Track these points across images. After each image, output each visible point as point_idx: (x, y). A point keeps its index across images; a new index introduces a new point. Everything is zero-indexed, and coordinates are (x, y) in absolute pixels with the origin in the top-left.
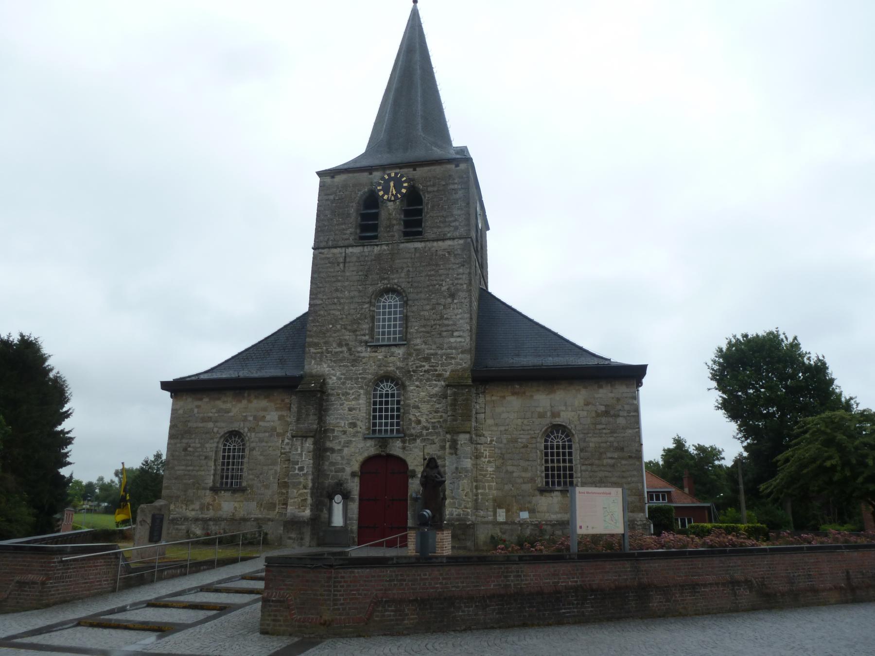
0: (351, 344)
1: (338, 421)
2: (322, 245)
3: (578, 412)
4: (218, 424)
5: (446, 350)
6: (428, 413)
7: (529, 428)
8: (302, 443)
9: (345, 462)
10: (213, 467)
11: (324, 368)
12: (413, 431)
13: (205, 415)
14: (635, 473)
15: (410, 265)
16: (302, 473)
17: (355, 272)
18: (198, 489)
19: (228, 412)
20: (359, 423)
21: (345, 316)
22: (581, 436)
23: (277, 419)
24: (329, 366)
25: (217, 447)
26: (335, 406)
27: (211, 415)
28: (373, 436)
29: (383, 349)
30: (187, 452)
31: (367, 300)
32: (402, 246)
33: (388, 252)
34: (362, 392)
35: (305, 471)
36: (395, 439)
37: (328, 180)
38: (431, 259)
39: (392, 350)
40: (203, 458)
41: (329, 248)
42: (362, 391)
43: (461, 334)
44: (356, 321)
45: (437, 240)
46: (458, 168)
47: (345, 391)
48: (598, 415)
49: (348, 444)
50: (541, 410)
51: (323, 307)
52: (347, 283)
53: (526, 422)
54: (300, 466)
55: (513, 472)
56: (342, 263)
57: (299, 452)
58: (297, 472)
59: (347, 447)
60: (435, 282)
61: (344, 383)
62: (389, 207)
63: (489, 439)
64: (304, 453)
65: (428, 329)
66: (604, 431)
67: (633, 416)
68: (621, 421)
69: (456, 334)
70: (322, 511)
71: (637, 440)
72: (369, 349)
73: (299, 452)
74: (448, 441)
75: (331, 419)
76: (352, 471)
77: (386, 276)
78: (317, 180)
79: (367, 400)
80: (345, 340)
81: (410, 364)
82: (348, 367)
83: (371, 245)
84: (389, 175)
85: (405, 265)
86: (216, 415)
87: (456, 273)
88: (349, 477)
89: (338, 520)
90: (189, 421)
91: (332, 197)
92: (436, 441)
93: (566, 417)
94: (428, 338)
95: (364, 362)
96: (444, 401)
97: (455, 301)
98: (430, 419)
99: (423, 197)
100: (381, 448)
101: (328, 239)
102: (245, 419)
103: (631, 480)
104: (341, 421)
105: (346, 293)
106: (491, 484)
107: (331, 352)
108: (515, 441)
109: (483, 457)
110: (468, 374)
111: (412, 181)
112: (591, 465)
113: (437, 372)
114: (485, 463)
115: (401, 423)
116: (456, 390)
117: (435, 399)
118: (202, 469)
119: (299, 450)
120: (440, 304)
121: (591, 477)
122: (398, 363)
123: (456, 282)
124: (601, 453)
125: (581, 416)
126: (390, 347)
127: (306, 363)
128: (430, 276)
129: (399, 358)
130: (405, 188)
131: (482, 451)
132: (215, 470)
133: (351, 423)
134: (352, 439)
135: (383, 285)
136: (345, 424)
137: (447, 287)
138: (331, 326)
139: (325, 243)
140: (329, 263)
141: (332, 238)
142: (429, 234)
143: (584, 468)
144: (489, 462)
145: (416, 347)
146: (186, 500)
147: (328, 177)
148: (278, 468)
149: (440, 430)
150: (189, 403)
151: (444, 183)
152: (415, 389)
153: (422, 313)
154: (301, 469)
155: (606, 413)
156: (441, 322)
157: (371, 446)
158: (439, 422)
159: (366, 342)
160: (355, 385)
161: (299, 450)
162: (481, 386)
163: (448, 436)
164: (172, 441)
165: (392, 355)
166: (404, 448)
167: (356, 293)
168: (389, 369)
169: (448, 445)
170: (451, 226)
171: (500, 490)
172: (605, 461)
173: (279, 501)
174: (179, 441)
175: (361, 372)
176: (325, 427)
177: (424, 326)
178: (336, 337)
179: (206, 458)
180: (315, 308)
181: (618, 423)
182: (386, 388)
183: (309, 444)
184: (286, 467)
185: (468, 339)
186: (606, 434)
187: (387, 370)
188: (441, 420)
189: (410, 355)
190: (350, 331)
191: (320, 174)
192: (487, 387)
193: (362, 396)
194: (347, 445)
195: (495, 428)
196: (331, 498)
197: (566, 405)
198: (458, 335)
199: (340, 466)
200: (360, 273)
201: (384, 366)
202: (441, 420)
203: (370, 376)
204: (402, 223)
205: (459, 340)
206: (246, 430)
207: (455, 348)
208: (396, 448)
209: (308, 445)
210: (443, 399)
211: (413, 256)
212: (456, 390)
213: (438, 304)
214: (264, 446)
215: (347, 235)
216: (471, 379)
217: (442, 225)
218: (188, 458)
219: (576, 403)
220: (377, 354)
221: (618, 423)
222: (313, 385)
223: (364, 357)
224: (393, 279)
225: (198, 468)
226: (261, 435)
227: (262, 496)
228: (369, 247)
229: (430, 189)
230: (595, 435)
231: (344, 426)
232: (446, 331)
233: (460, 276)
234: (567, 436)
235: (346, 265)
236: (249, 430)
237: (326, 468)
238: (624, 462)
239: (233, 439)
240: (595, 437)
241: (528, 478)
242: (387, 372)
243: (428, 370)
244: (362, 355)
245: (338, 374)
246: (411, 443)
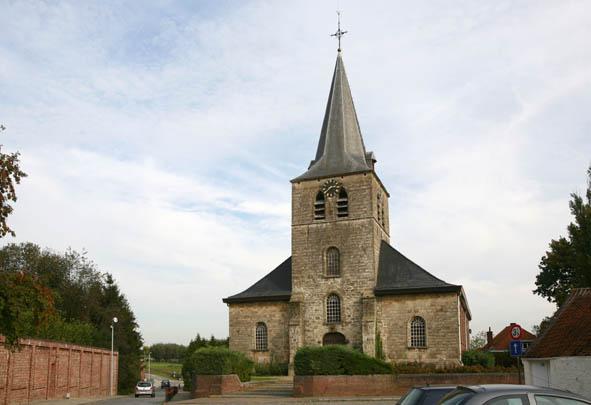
11: (302, 290)
78: (291, 185)
93: (422, 313)
108: (396, 324)
142: (352, 215)
150: (237, 309)
155: (441, 310)
208: (339, 329)
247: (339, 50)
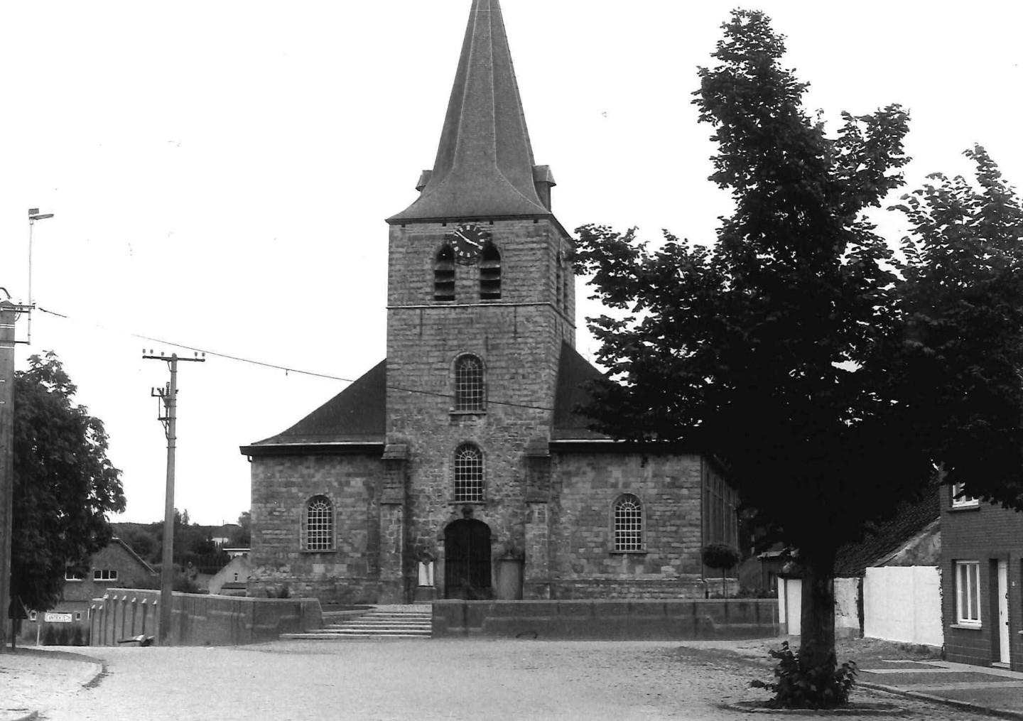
46: (536, 224)
84: (464, 228)
93: (634, 487)
115: (484, 490)
123: (534, 351)
140: (406, 325)
172: (669, 529)
208: (480, 515)
233: (539, 346)
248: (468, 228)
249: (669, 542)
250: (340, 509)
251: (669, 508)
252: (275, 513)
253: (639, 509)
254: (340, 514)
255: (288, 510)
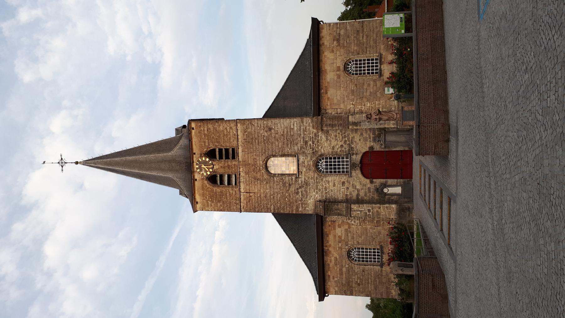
0: (297, 186)
1: (341, 192)
2: (238, 207)
3: (337, 56)
4: (344, 264)
5: (301, 132)
6: (337, 141)
7: (345, 84)
8: (354, 211)
9: (364, 187)
10: (369, 267)
12: (347, 149)
13: (338, 273)
14: (371, 24)
15: (252, 154)
16: (371, 210)
17: (255, 186)
18: (382, 275)
19: (337, 259)
20: (343, 180)
21: (281, 191)
22: (350, 54)
23: (340, 229)
24: (310, 199)
25: (357, 265)
26: (333, 194)
27: (338, 270)
28: (350, 172)
29: (300, 168)
30: (361, 283)
31: (272, 178)
32: (240, 159)
33: (244, 168)
34: (325, 179)
35: (371, 208)
36: (351, 160)
37: (198, 206)
38: (249, 142)
39: (301, 163)
40: (363, 273)
41: (240, 203)
42: (324, 179)
43: (292, 124)
44: (284, 184)
45: (238, 139)
46: (195, 128)
47: (324, 189)
48: (339, 45)
49: (354, 186)
50: (336, 77)
51: (276, 204)
52: (262, 191)
53: (342, 86)
54: (367, 212)
55: (370, 92)
56: (250, 194)
57: (359, 212)
58: (371, 213)
59: (356, 186)
60: (262, 139)
61: (320, 190)
62: (217, 168)
63: (352, 106)
64: (360, 210)
65: (289, 142)
66: (348, 41)
67: (340, 25)
68: (342, 32)
69: (292, 127)
70: (393, 199)
71: (353, 23)
72: (300, 176)
73: (359, 212)
74: (353, 127)
75: (340, 197)
76: (370, 183)
77: (258, 168)
79: (329, 176)
80: (295, 190)
81: (309, 152)
82: (310, 188)
83: (240, 178)
84: (197, 169)
85: (252, 157)
86: (338, 266)
87: (257, 128)
88: (373, 185)
89: (398, 190)
90: (342, 283)
91: (209, 202)
92: (352, 136)
93: (340, 63)
94: (294, 143)
95: (307, 178)
96: (330, 132)
97: (273, 128)
98: (340, 139)
99: (212, 148)
100: (357, 167)
101: (235, 203)
102: (341, 248)
103: (375, 26)
104: (341, 191)
105: (267, 191)
106: (377, 104)
107: (302, 198)
108: (353, 91)
109: (361, 109)
110: (315, 119)
111: (201, 155)
112: (366, 48)
113: (314, 137)
114: (365, 108)
116: (324, 125)
117: (329, 137)
118: (370, 273)
119: (358, 212)
120: (275, 136)
121: (373, 48)
122: (309, 159)
123: (262, 127)
124: (360, 43)
125: (339, 55)
126: (299, 164)
127: (308, 213)
128: (258, 142)
129: (306, 158)
130: (205, 159)
131: (358, 109)
132: (371, 265)
133: (343, 185)
134: (351, 184)
135: (263, 169)
136: (342, 188)
137: (265, 133)
138: (287, 199)
139: (237, 205)
140: (250, 202)
141: (235, 201)
142: (234, 144)
143: (368, 52)
144: (364, 105)
145: (299, 149)
146: (388, 282)
147: (197, 205)
148: (369, 227)
149: (346, 134)
150: (331, 284)
151: (204, 136)
152: (323, 149)
153: (280, 147)
154: (369, 211)
155: (338, 40)
156: (286, 136)
157: (355, 173)
158: (342, 134)
159: (296, 178)
160: (321, 183)
161: (358, 212)
162: (322, 112)
163: (350, 127)
164: (354, 293)
165: (303, 162)
166: (357, 154)
167: (268, 185)
168: (312, 164)
169: (355, 127)
170: (230, 131)
171: (380, 99)
173: (388, 225)
174: (354, 289)
175: (313, 180)
176: (344, 200)
177: (287, 145)
178: (293, 196)
179: (363, 271)
180: (276, 209)
181: (343, 34)
182: (323, 164)
183: (354, 207)
184: (368, 222)
185: (295, 120)
186: (349, 40)
187: (312, 165)
188: (341, 133)
189: (304, 152)
190: (289, 188)
191: (195, 211)
192: (322, 108)
193: (327, 179)
194: (355, 187)
195: (346, 103)
196: (386, 194)
197: (333, 63)
198: (293, 126)
199: (367, 190)
200: (256, 183)
201: (310, 167)
202: (341, 133)
203: (316, 175)
204: (227, 160)
205: (295, 125)
206: (347, 247)
207: (300, 127)
208: (357, 158)
209: (355, 207)
210: (329, 133)
211: (247, 153)
212: (324, 125)
213: (275, 137)
214: (356, 236)
215: (233, 192)
216: (318, 117)
217: (229, 137)
218: (364, 282)
219: (333, 57)
220: (303, 172)
221: (343, 34)
222: (321, 207)
223: (305, 179)
224: (260, 164)
225: (370, 276)
226: (350, 238)
227: (385, 236)
228: (240, 179)
229: (207, 144)
230: (350, 47)
231: (344, 189)
232: (290, 133)
233: (259, 125)
234: (350, 63)
235: (251, 192)
236: (347, 245)
237: (368, 198)
238: (365, 30)
239: (352, 253)
240: (351, 46)
241: (373, 83)
242: (313, 165)
243: (312, 142)
244: (303, 180)
245: (315, 194)
246: (353, 150)
247: (77, 163)
248: (197, 167)
249: (373, 40)
250: (355, 242)
251: (352, 42)
252: (358, 282)
253: (353, 61)
254: (358, 242)
255: (357, 274)
